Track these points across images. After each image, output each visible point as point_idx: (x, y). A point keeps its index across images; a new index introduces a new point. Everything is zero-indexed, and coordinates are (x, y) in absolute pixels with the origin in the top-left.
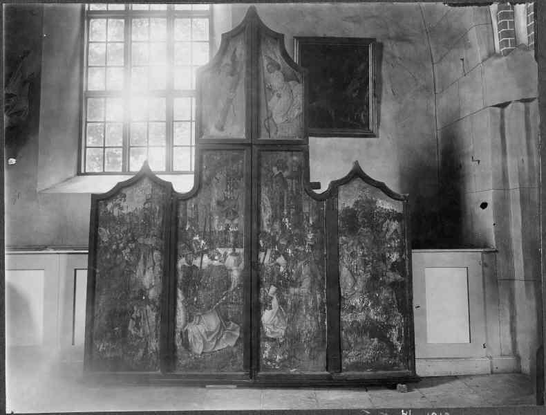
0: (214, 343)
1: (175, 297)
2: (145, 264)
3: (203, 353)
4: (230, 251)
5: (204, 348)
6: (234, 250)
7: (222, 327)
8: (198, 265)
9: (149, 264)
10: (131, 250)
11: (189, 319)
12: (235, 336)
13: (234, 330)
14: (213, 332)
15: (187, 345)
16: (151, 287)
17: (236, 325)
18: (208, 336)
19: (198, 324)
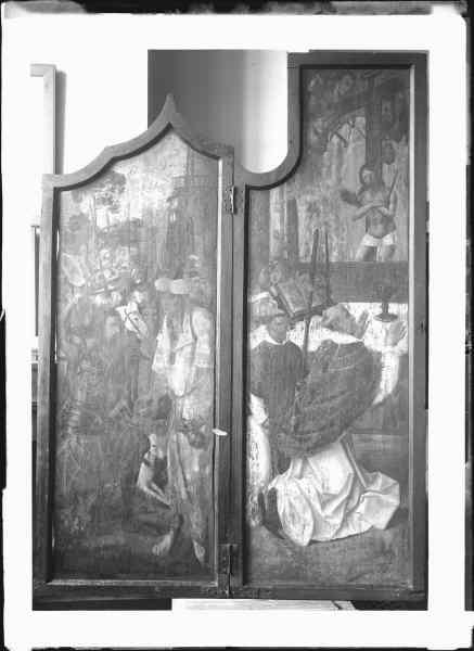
0: (337, 521)
1: (246, 412)
2: (174, 338)
3: (312, 542)
4: (375, 309)
5: (315, 531)
6: (385, 308)
7: (356, 486)
8: (300, 343)
9: (185, 338)
10: (140, 308)
11: (279, 465)
12: (388, 505)
13: (386, 491)
14: (335, 497)
15: (273, 523)
16: (192, 390)
17: (391, 481)
18: (324, 505)
19: (301, 477)
